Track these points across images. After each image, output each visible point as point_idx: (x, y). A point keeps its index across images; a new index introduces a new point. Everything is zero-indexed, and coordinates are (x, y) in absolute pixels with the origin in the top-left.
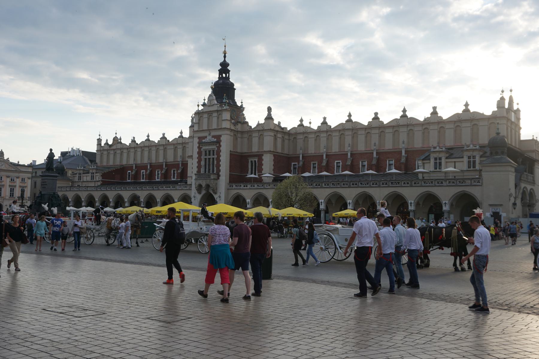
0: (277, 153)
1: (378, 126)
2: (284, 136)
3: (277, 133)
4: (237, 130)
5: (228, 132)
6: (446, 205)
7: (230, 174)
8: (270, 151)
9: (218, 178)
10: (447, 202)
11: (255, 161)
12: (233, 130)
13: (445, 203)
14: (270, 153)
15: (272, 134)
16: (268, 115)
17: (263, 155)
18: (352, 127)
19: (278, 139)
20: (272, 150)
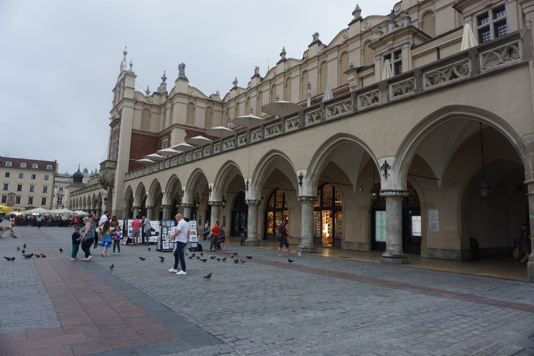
0: (195, 128)
1: (317, 54)
2: (212, 106)
3: (196, 101)
4: (151, 103)
5: (132, 104)
6: (389, 171)
7: (130, 160)
8: (178, 125)
9: (116, 168)
10: (391, 161)
11: (166, 141)
12: (143, 102)
13: (386, 166)
14: (177, 127)
15: (186, 101)
16: (180, 74)
17: (170, 132)
18: (285, 69)
19: (197, 109)
20: (184, 122)
